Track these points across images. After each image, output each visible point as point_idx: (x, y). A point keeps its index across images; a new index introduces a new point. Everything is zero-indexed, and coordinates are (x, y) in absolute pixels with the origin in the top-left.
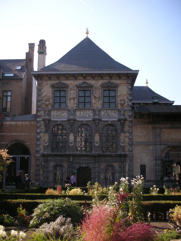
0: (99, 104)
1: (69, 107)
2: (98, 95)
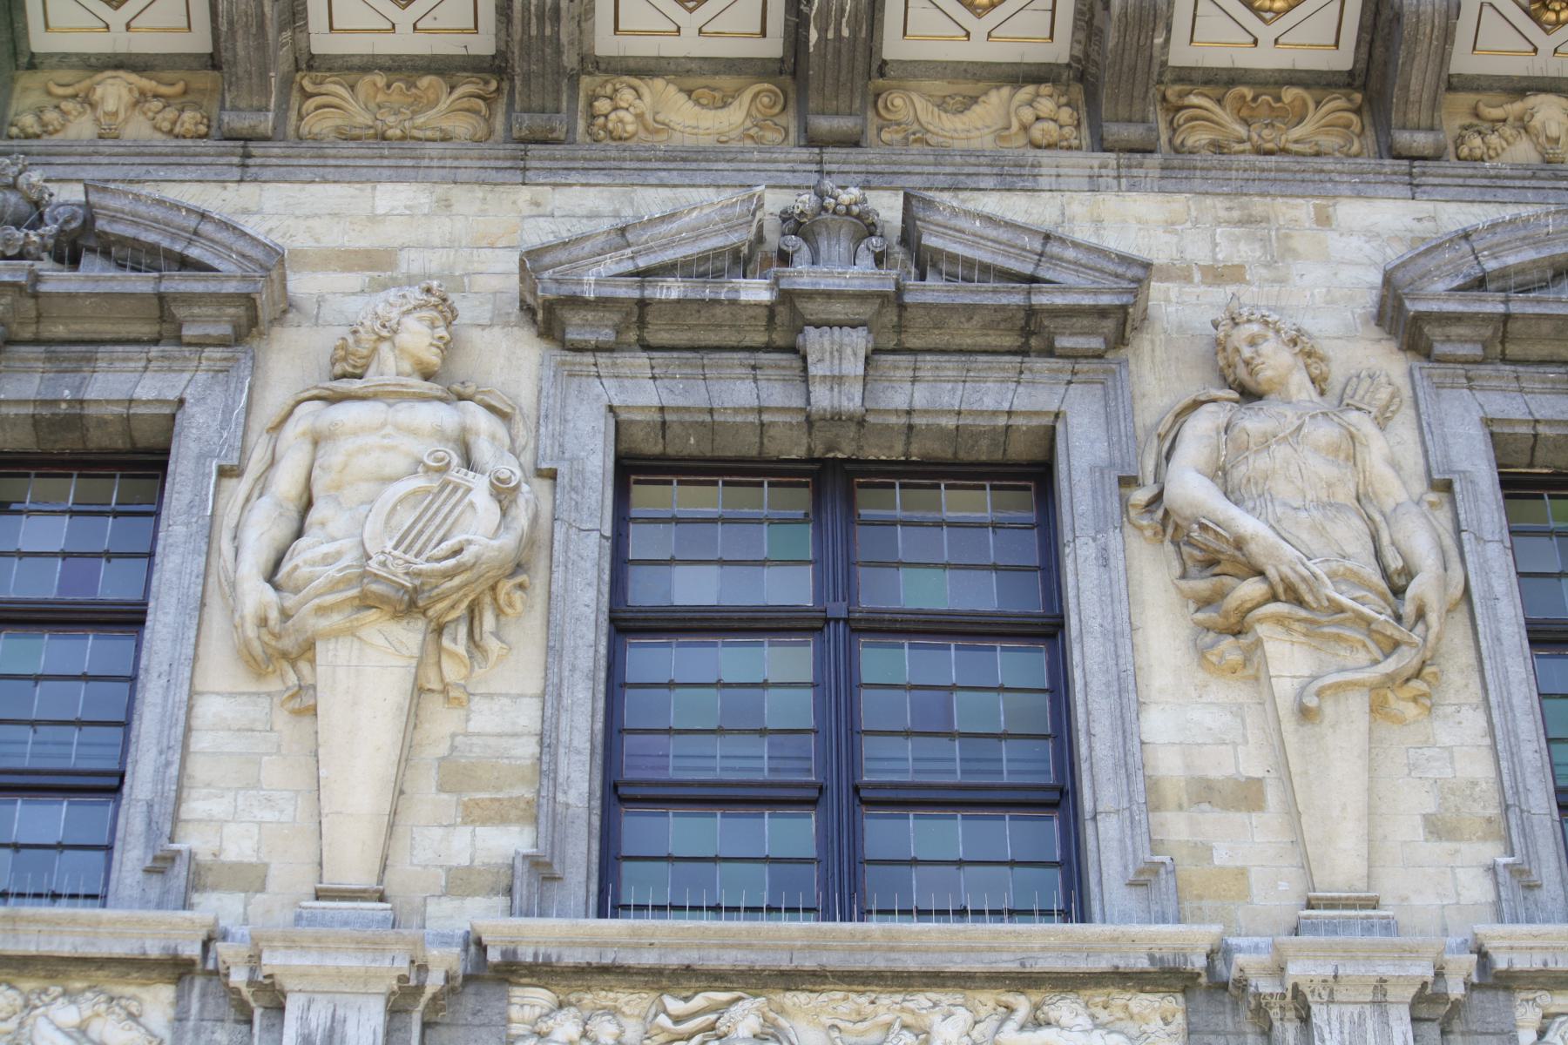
0: (1406, 829)
1: (251, 878)
2: (1350, 536)
